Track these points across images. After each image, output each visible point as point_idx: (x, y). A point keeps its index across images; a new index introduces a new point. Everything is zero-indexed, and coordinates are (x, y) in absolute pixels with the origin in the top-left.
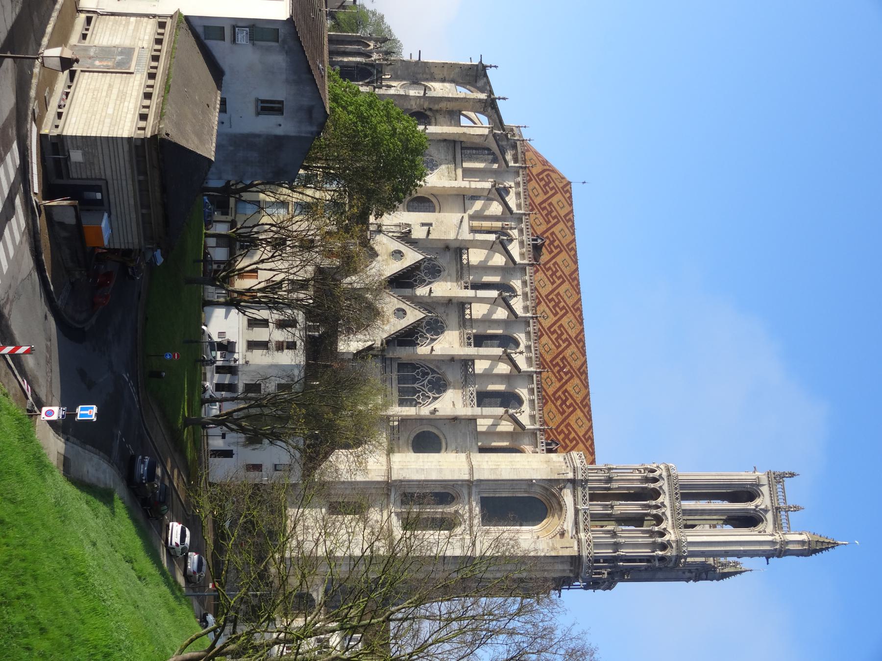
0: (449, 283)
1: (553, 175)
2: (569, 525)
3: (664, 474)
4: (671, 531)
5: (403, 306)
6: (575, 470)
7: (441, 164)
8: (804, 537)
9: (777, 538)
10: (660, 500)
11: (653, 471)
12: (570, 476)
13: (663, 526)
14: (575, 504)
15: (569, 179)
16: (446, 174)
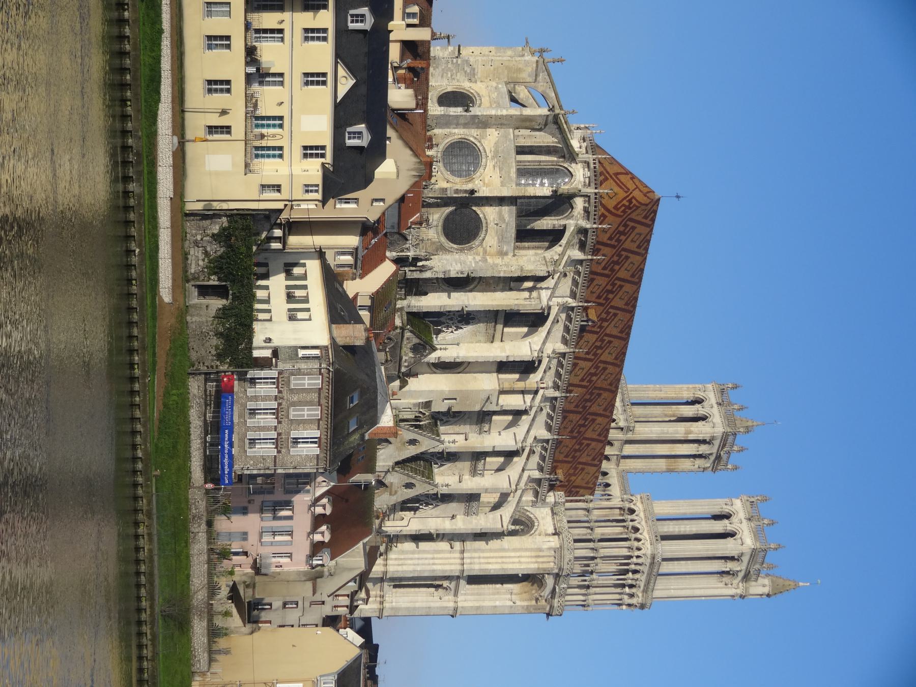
0: (468, 427)
1: (633, 216)
2: (547, 592)
3: (649, 561)
4: (640, 595)
5: (413, 481)
6: (560, 569)
7: (479, 322)
8: (766, 590)
9: (739, 591)
10: (637, 576)
11: (638, 557)
12: (556, 571)
13: (634, 590)
14: (555, 583)
15: (658, 194)
16: (484, 330)
